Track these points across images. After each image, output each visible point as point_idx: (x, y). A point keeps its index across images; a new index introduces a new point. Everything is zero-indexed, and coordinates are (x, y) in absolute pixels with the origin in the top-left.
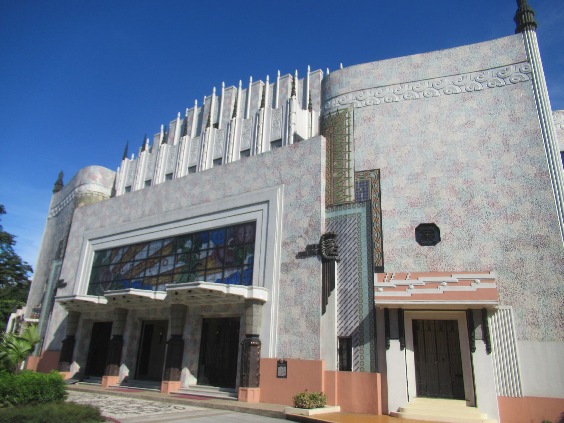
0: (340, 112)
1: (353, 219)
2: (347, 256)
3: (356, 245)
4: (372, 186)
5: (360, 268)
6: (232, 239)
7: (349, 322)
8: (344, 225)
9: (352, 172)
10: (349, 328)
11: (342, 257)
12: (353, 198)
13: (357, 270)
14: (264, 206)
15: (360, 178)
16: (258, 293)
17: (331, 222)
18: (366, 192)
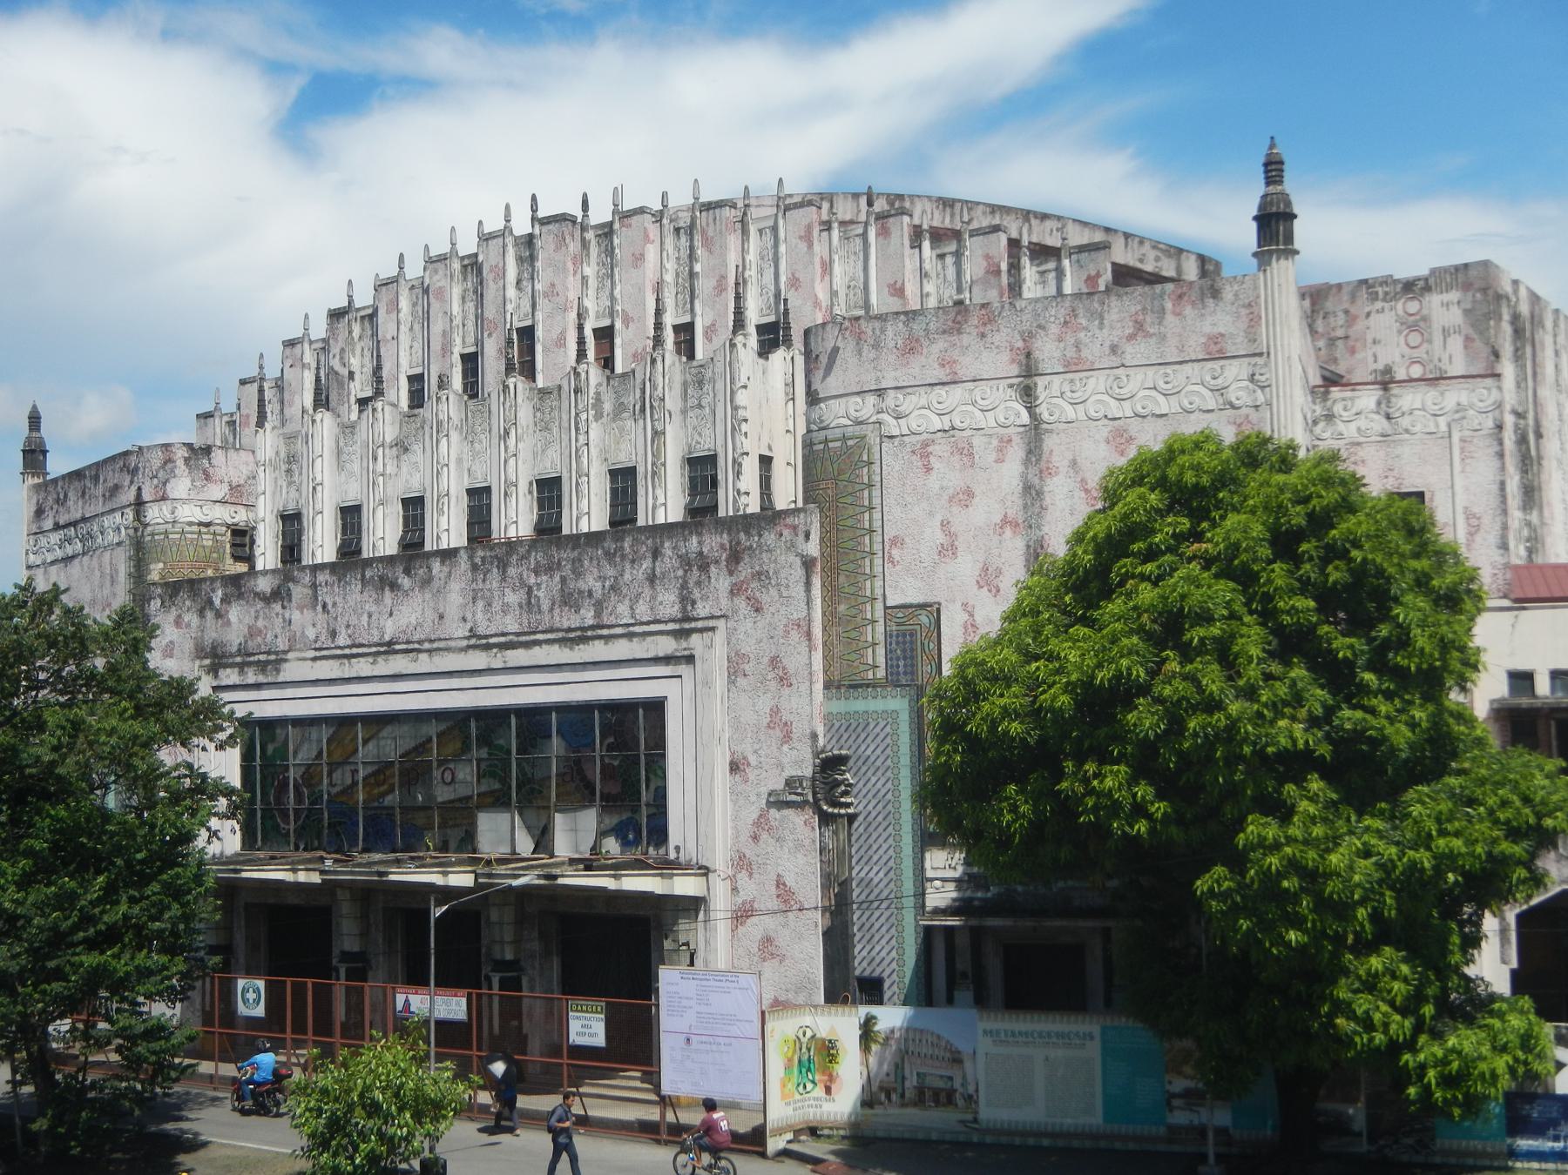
0: (850, 443)
1: (882, 724)
2: (870, 807)
3: (889, 785)
4: (923, 649)
5: (898, 837)
6: (611, 740)
7: (877, 948)
8: (863, 736)
9: (879, 606)
10: (878, 960)
11: (860, 807)
12: (881, 673)
13: (891, 841)
14: (682, 669)
15: (899, 624)
16: (685, 886)
17: (837, 725)
18: (910, 656)
